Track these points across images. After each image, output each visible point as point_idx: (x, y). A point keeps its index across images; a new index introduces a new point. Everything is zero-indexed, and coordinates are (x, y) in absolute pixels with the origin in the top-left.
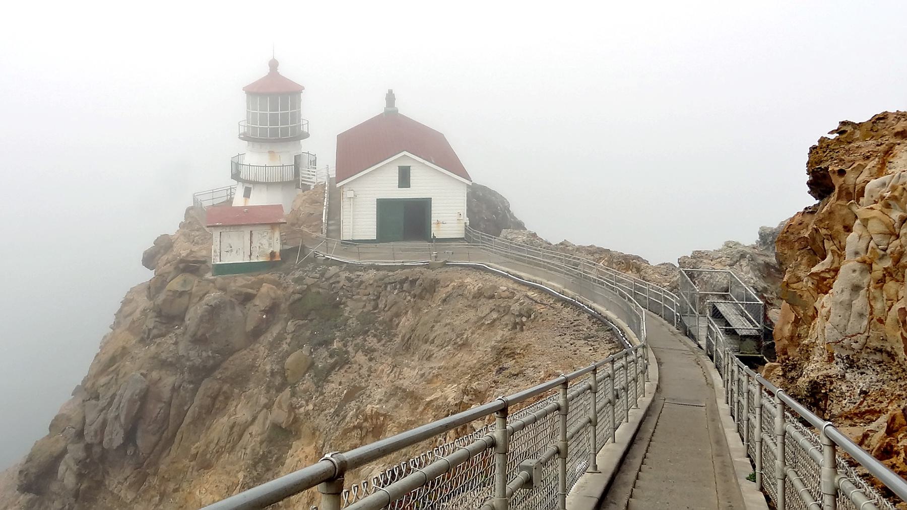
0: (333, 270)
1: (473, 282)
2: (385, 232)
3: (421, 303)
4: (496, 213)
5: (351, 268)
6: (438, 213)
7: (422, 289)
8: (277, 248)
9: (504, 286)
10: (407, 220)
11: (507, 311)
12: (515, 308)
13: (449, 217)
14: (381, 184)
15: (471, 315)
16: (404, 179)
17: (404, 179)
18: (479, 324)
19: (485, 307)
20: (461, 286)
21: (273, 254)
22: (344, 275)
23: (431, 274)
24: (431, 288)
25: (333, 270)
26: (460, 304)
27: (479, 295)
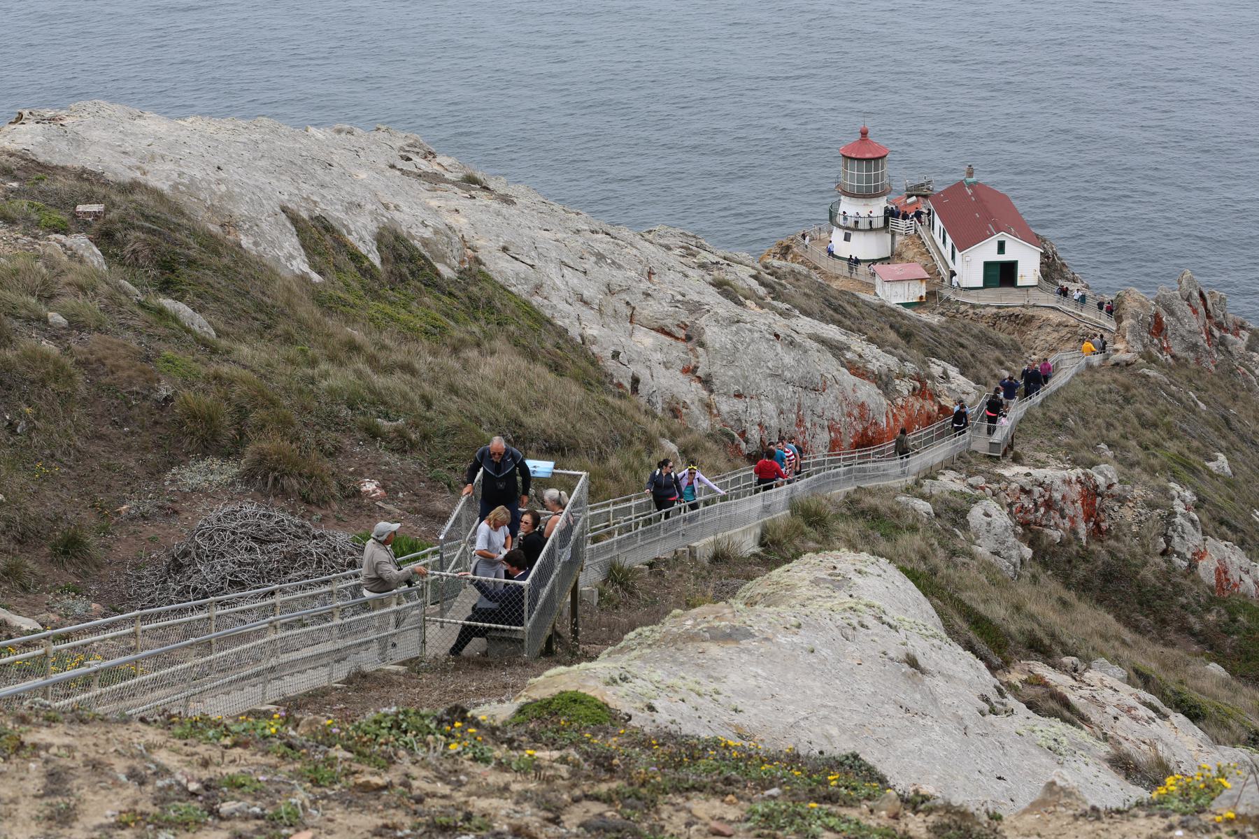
0: (963, 308)
1: (1055, 317)
2: (987, 283)
3: (1024, 328)
4: (1048, 257)
5: (973, 306)
6: (1020, 270)
7: (1021, 321)
8: (924, 294)
9: (1072, 322)
10: (1003, 274)
11: (1075, 333)
12: (1081, 332)
13: (1029, 272)
14: (987, 251)
15: (1055, 335)
16: (1001, 248)
17: (1001, 248)
18: (1061, 340)
19: (1064, 331)
20: (1048, 319)
21: (921, 297)
22: (971, 311)
23: (1030, 312)
24: (1029, 320)
25: (963, 308)
26: (1049, 329)
27: (1059, 324)
